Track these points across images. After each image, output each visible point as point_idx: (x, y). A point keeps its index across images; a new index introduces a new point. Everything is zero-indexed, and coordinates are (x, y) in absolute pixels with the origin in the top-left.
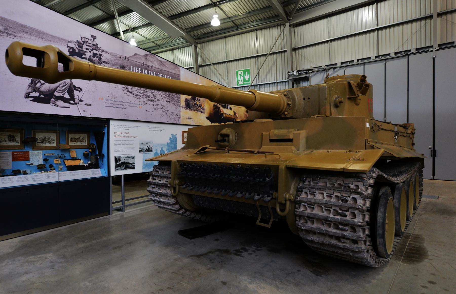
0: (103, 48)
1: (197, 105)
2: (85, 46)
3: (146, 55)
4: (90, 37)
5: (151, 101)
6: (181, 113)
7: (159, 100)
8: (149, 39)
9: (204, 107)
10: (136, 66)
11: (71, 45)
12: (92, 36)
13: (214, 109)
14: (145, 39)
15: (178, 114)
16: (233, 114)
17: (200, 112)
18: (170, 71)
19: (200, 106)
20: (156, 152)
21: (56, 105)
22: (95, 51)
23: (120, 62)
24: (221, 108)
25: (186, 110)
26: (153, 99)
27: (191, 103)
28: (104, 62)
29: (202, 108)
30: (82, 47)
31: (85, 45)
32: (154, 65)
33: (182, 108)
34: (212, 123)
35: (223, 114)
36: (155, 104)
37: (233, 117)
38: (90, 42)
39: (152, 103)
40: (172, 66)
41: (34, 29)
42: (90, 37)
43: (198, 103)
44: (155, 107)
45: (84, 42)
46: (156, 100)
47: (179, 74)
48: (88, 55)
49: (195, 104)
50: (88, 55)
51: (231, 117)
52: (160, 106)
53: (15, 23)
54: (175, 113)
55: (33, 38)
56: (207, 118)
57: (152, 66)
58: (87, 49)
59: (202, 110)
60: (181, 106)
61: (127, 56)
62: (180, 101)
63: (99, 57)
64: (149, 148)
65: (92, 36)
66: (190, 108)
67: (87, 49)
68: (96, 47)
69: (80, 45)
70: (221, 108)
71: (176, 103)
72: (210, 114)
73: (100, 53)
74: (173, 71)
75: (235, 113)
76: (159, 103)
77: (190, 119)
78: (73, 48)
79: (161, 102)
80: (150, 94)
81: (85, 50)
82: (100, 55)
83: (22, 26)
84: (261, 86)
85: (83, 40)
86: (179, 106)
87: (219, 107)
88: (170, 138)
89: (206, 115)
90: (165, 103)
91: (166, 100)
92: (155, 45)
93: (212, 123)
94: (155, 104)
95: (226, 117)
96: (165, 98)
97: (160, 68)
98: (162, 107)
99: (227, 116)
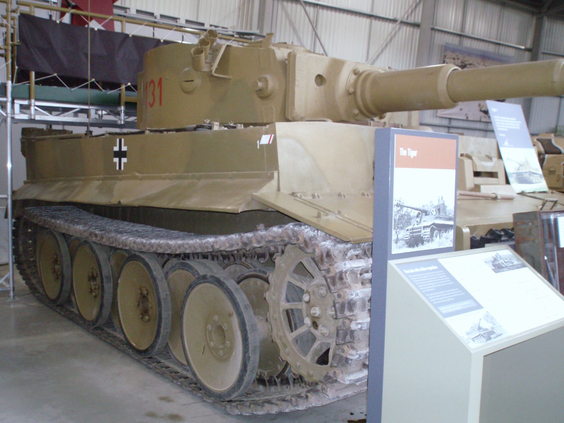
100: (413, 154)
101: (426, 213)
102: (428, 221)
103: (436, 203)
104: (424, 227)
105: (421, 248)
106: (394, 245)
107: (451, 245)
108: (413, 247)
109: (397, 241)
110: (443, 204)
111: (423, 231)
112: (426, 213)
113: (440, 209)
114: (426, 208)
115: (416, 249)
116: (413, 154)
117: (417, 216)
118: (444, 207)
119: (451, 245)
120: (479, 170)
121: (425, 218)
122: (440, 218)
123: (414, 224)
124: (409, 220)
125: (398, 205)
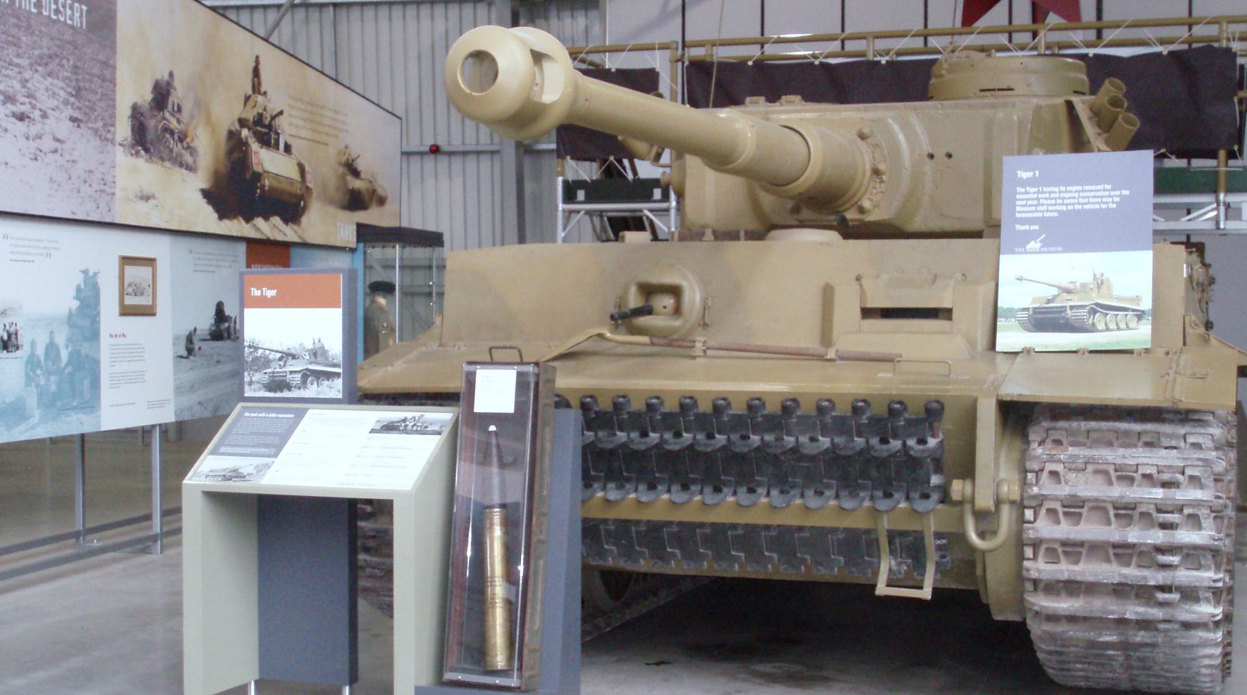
1: (172, 133)
5: (21, 117)
6: (117, 172)
7: (44, 116)
9: (195, 144)
13: (230, 152)
15: (109, 178)
16: (294, 174)
17: (181, 165)
19: (181, 140)
20: (32, 355)
24: (255, 146)
25: (133, 160)
26: (25, 108)
27: (151, 124)
29: (189, 147)
33: (119, 150)
34: (221, 218)
35: (257, 177)
36: (34, 130)
37: (297, 189)
39: (21, 127)
43: (174, 124)
44: (33, 145)
46: (36, 114)
49: (166, 129)
51: (284, 186)
52: (48, 143)
54: (98, 175)
56: (206, 194)
59: (188, 158)
60: (119, 138)
62: (113, 116)
64: (9, 336)
66: (147, 150)
70: (255, 146)
71: (99, 124)
72: (217, 177)
75: (301, 168)
76: (47, 129)
77: (147, 198)
79: (50, 121)
80: (17, 86)
84: (343, 13)
86: (113, 142)
87: (246, 144)
88: (79, 290)
89: (200, 180)
90: (63, 128)
91: (69, 112)
93: (221, 218)
94: (34, 130)
95: (272, 189)
96: (66, 103)
98: (57, 145)
99: (275, 184)
100: (271, 293)
101: (294, 357)
102: (298, 366)
103: (310, 346)
104: (291, 372)
105: (286, 394)
106: (247, 388)
107: (340, 396)
108: (275, 391)
109: (251, 383)
110: (322, 347)
111: (289, 376)
112: (294, 357)
113: (317, 353)
114: (293, 351)
115: (278, 395)
116: (271, 293)
117: (280, 359)
118: (324, 352)
119: (340, 396)
120: (869, 305)
121: (290, 361)
122: (318, 364)
123: (275, 368)
124: (267, 363)
125: (250, 347)
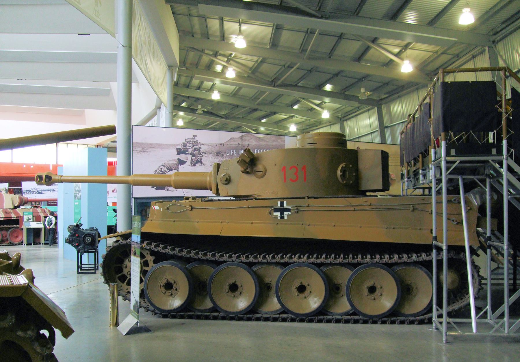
0: (202, 142)
2: (188, 145)
3: (242, 136)
4: (191, 137)
8: (437, 52)
10: (231, 148)
11: (178, 147)
12: (193, 136)
14: (431, 53)
18: (271, 144)
21: (169, 190)
22: (195, 147)
23: (217, 149)
28: (203, 153)
30: (186, 146)
31: (188, 144)
32: (250, 143)
38: (191, 141)
40: (274, 138)
41: (157, 144)
42: (191, 137)
45: (187, 142)
47: (282, 143)
48: (190, 150)
50: (190, 150)
53: (147, 144)
55: (156, 149)
57: (248, 145)
58: (189, 147)
61: (223, 142)
63: (199, 150)
65: (193, 136)
67: (189, 147)
68: (196, 143)
69: (185, 145)
73: (200, 146)
74: (274, 143)
78: (180, 149)
81: (188, 148)
82: (200, 148)
83: (151, 144)
85: (187, 141)
92: (449, 57)
97: (257, 144)
